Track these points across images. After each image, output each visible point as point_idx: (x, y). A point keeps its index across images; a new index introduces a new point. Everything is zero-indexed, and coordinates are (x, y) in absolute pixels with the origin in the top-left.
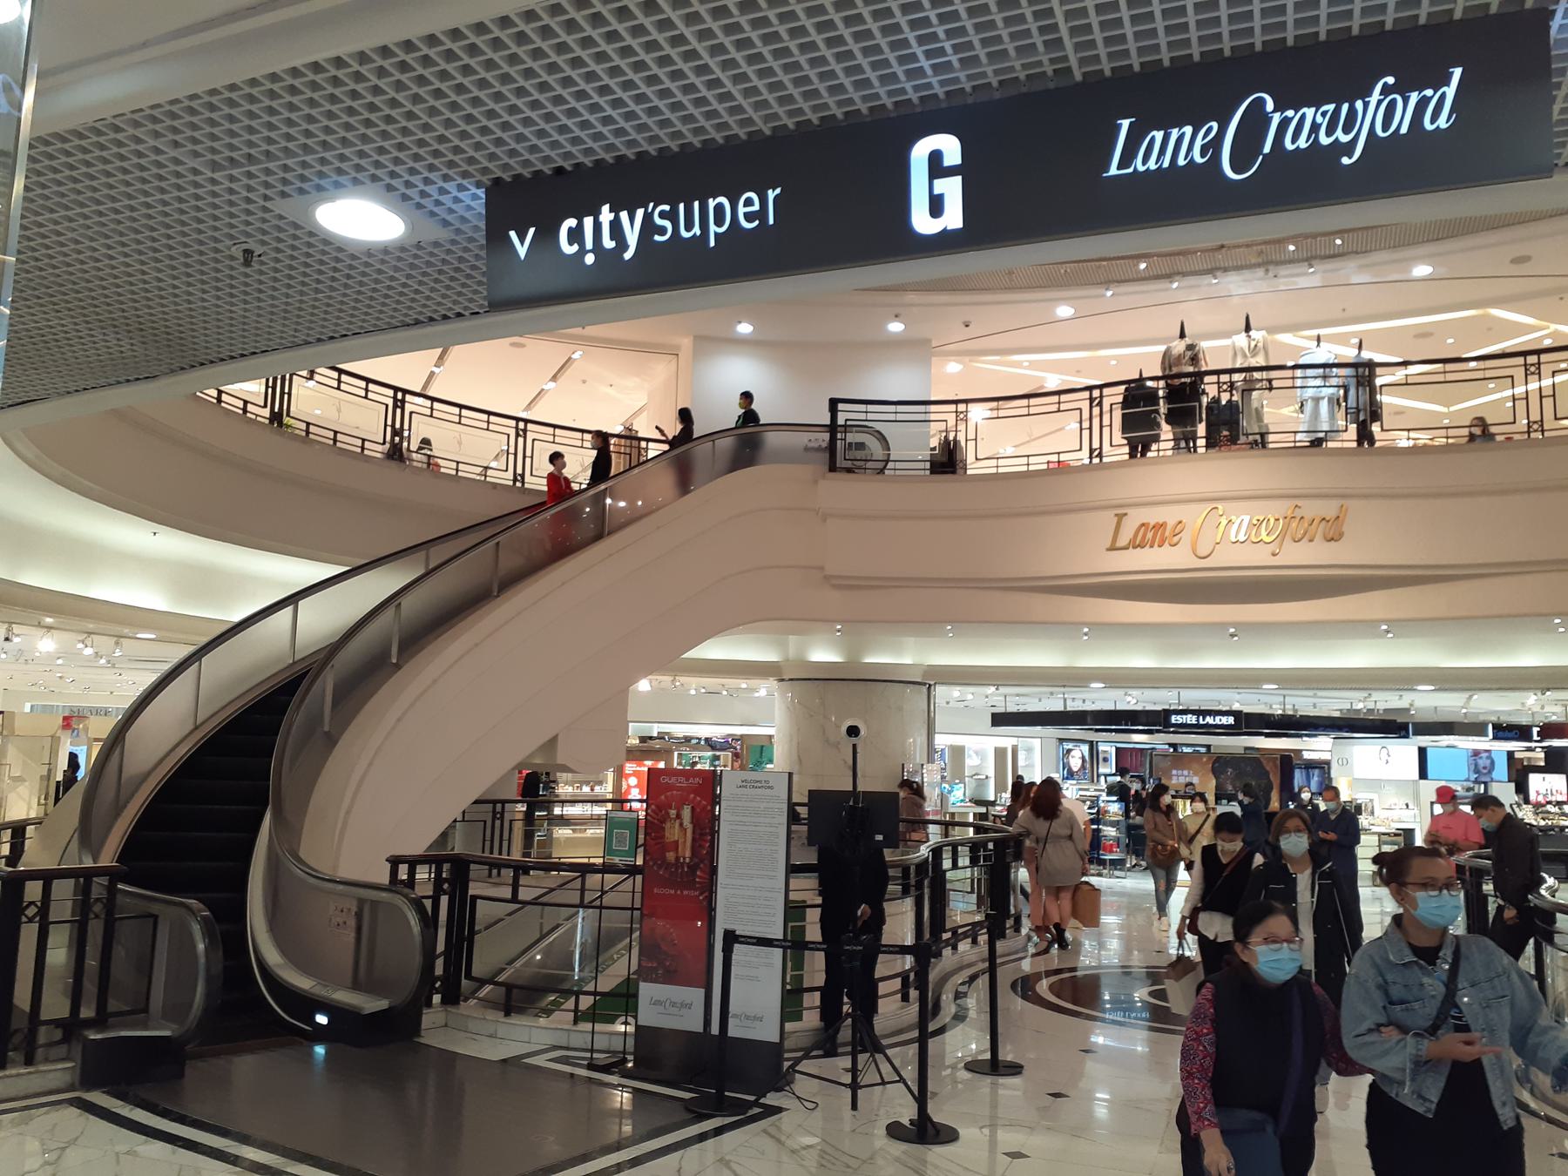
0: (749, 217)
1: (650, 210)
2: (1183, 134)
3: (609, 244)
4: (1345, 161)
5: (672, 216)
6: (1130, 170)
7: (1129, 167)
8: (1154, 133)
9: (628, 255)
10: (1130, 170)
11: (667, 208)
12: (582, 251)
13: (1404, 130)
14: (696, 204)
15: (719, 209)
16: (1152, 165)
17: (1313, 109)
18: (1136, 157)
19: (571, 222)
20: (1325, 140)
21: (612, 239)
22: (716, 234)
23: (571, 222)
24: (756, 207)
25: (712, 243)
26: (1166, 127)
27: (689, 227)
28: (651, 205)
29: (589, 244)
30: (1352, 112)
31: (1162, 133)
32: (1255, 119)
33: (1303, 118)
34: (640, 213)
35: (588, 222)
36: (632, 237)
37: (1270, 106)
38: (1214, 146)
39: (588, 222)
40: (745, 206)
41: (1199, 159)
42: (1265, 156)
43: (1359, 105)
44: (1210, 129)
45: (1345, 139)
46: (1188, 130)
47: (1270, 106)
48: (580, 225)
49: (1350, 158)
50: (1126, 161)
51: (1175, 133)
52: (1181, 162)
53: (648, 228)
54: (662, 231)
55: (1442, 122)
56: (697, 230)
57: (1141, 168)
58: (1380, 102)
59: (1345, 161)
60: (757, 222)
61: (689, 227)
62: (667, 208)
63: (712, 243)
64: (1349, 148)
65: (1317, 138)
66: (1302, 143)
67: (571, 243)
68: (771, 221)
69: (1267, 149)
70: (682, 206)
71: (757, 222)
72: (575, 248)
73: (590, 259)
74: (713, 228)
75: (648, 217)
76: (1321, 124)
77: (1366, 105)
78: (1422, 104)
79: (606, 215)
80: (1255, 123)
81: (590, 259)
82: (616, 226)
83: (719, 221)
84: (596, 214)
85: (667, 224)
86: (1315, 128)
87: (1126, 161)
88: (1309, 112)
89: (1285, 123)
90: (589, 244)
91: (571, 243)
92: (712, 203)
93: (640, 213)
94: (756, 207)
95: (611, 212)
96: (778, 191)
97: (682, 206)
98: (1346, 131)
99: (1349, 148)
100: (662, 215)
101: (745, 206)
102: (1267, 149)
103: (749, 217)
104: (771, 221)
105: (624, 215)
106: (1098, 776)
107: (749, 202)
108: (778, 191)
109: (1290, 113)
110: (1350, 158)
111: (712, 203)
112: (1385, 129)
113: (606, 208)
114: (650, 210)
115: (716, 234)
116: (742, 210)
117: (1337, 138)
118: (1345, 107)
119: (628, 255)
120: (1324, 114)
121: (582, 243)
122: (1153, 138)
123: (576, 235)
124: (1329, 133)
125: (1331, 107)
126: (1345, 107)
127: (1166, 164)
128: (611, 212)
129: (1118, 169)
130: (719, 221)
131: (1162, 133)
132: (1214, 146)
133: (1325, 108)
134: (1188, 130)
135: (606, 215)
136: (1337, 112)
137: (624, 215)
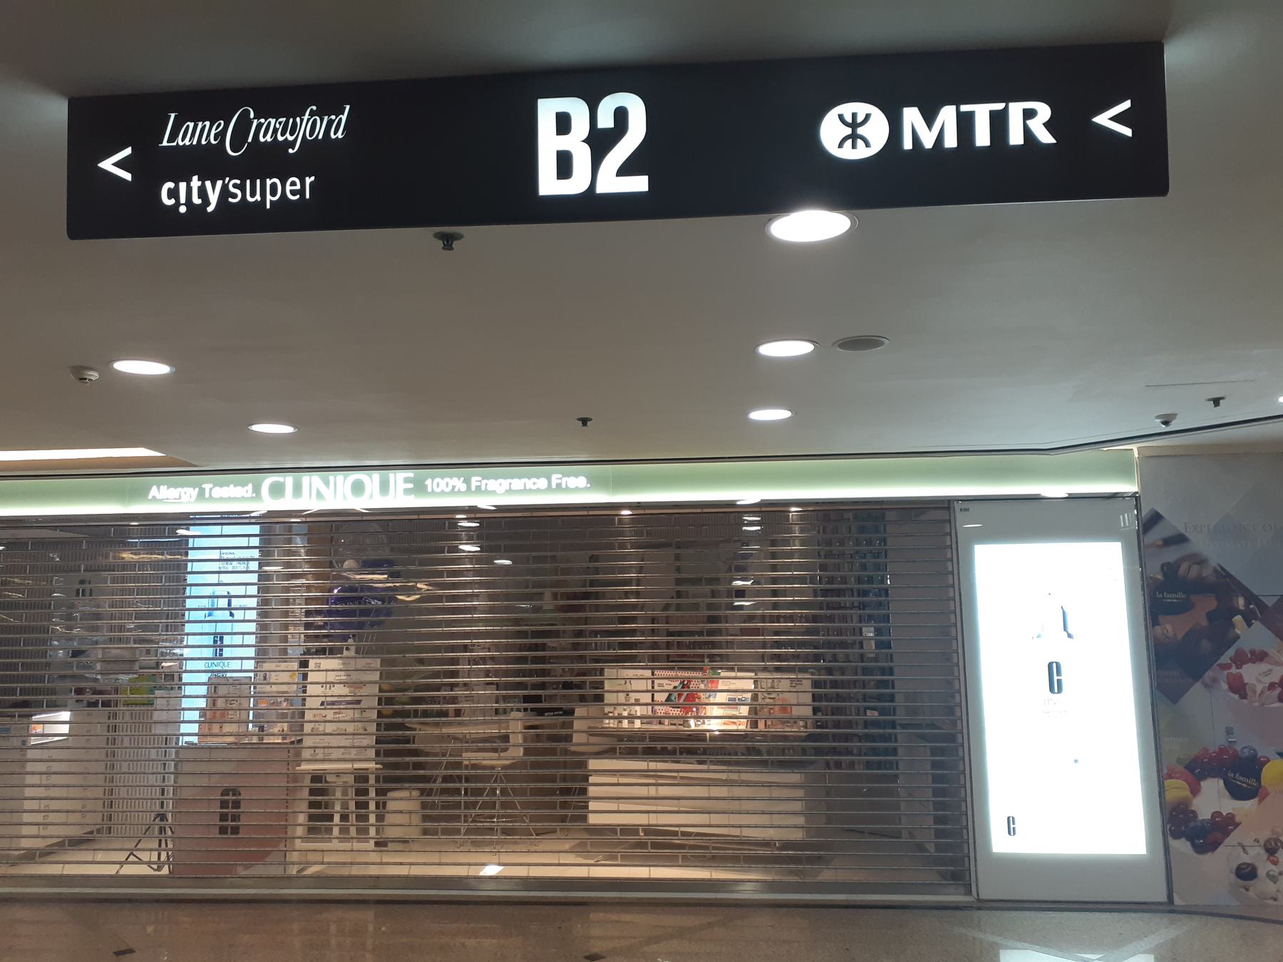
0: (293, 193)
1: (226, 182)
2: (205, 126)
3: (196, 200)
4: (291, 151)
5: (242, 187)
6: (175, 144)
7: (174, 142)
8: (189, 123)
9: (210, 209)
10: (175, 144)
11: (238, 182)
12: (178, 204)
13: (320, 137)
14: (258, 181)
15: (274, 186)
16: (187, 142)
17: (274, 120)
18: (178, 136)
19: (170, 185)
20: (280, 138)
21: (199, 198)
22: (271, 201)
23: (170, 185)
24: (298, 187)
25: (268, 207)
26: (196, 122)
27: (253, 195)
28: (227, 179)
29: (183, 199)
30: (295, 123)
31: (193, 123)
32: (243, 125)
33: (269, 124)
34: (219, 183)
35: (183, 186)
36: (214, 198)
37: (252, 115)
38: (221, 135)
39: (183, 186)
40: (291, 185)
41: (213, 142)
42: (249, 143)
43: (298, 120)
44: (220, 124)
45: (291, 138)
46: (208, 123)
47: (252, 115)
48: (177, 187)
49: (293, 149)
50: (173, 137)
51: (200, 124)
52: (203, 142)
53: (225, 193)
54: (235, 196)
55: (340, 135)
56: (258, 197)
57: (181, 143)
58: (308, 120)
59: (291, 151)
60: (298, 196)
61: (253, 195)
62: (238, 182)
63: (268, 207)
64: (292, 144)
65: (276, 136)
66: (269, 138)
67: (169, 198)
68: (308, 197)
69: (250, 140)
70: (248, 181)
71: (298, 196)
72: (172, 202)
73: (183, 209)
74: (269, 197)
75: (225, 187)
76: (278, 129)
77: (302, 121)
78: (330, 123)
79: (195, 183)
80: (243, 125)
81: (183, 209)
82: (203, 193)
83: (273, 193)
84: (189, 181)
85: (238, 192)
86: (275, 130)
87: (173, 137)
88: (273, 121)
89: (259, 126)
90: (183, 199)
91: (169, 198)
92: (269, 182)
93: (219, 183)
94: (298, 187)
95: (199, 180)
96: (313, 178)
97: (248, 181)
98: (291, 134)
99: (292, 144)
100: (235, 186)
101: (291, 185)
102: (250, 140)
103: (293, 193)
104: (308, 197)
105: (208, 184)
106: (653, 669)
107: (293, 184)
108: (313, 178)
109: (262, 120)
110: (293, 149)
111: (269, 182)
112: (311, 136)
113: (195, 178)
114: (226, 182)
115: (271, 201)
116: (288, 188)
117: (286, 138)
118: (291, 120)
119: (210, 209)
120: (280, 123)
121: (177, 198)
122: (188, 126)
123: (173, 193)
124: (283, 135)
125: (284, 119)
126: (291, 120)
127: (195, 143)
128: (199, 180)
129: (168, 142)
130: (273, 193)
131: (193, 123)
132: (221, 135)
133: (281, 120)
134: (208, 123)
135: (195, 183)
136: (287, 122)
137: (208, 184)
